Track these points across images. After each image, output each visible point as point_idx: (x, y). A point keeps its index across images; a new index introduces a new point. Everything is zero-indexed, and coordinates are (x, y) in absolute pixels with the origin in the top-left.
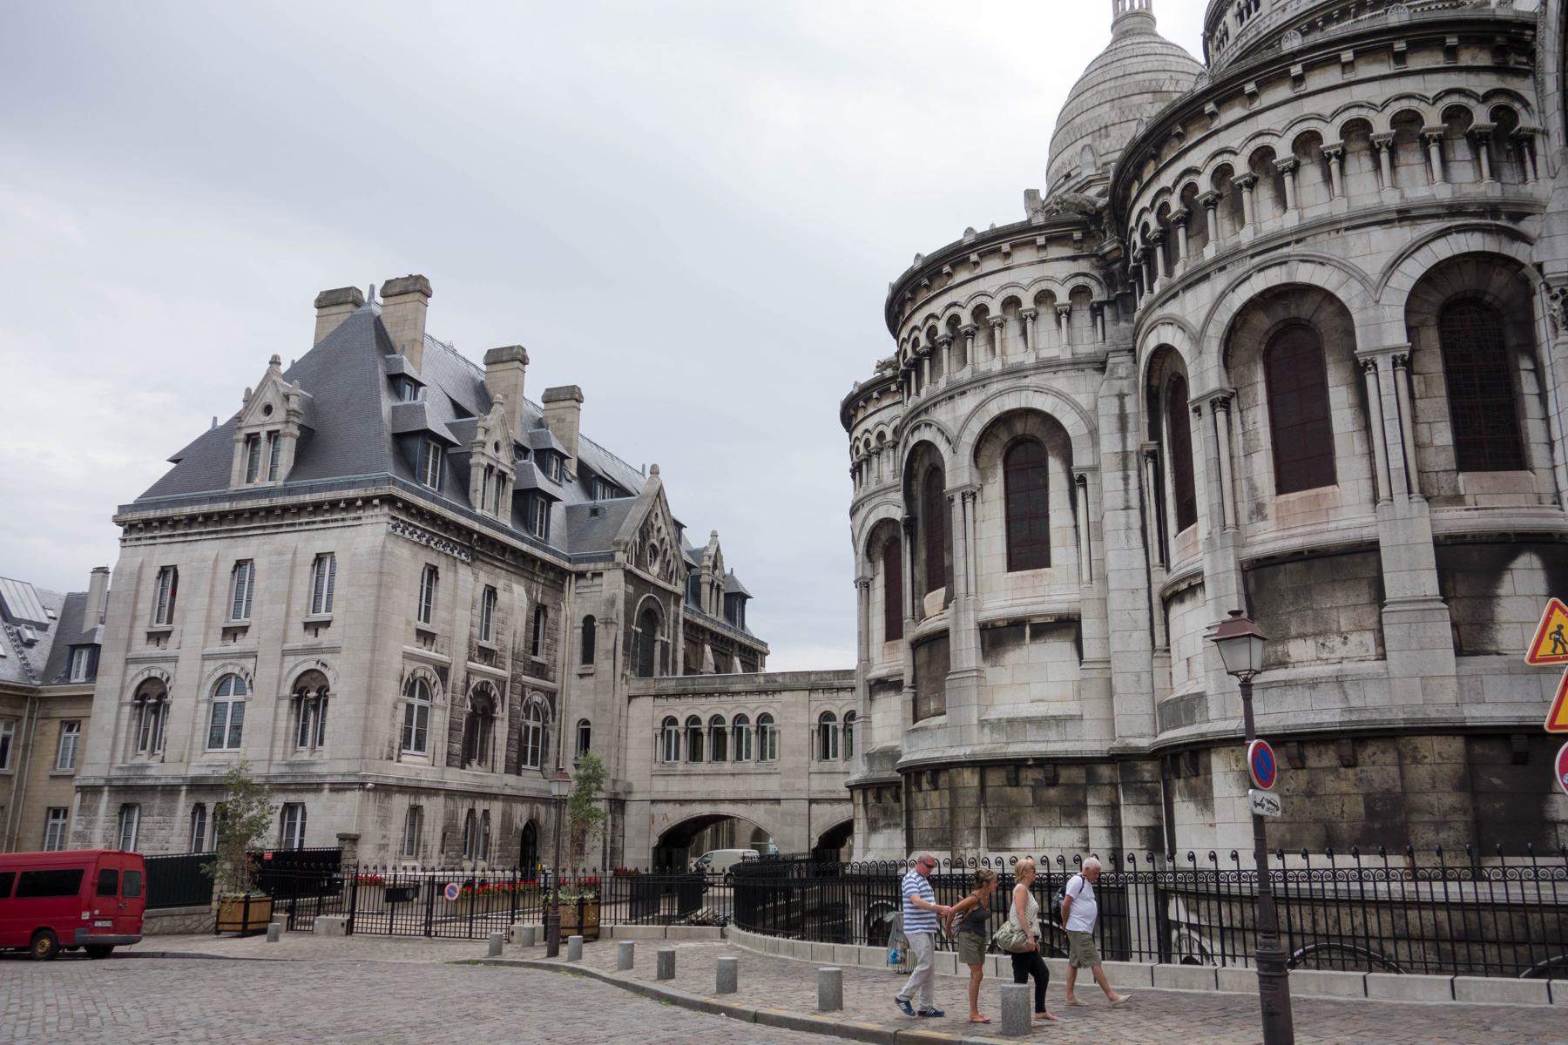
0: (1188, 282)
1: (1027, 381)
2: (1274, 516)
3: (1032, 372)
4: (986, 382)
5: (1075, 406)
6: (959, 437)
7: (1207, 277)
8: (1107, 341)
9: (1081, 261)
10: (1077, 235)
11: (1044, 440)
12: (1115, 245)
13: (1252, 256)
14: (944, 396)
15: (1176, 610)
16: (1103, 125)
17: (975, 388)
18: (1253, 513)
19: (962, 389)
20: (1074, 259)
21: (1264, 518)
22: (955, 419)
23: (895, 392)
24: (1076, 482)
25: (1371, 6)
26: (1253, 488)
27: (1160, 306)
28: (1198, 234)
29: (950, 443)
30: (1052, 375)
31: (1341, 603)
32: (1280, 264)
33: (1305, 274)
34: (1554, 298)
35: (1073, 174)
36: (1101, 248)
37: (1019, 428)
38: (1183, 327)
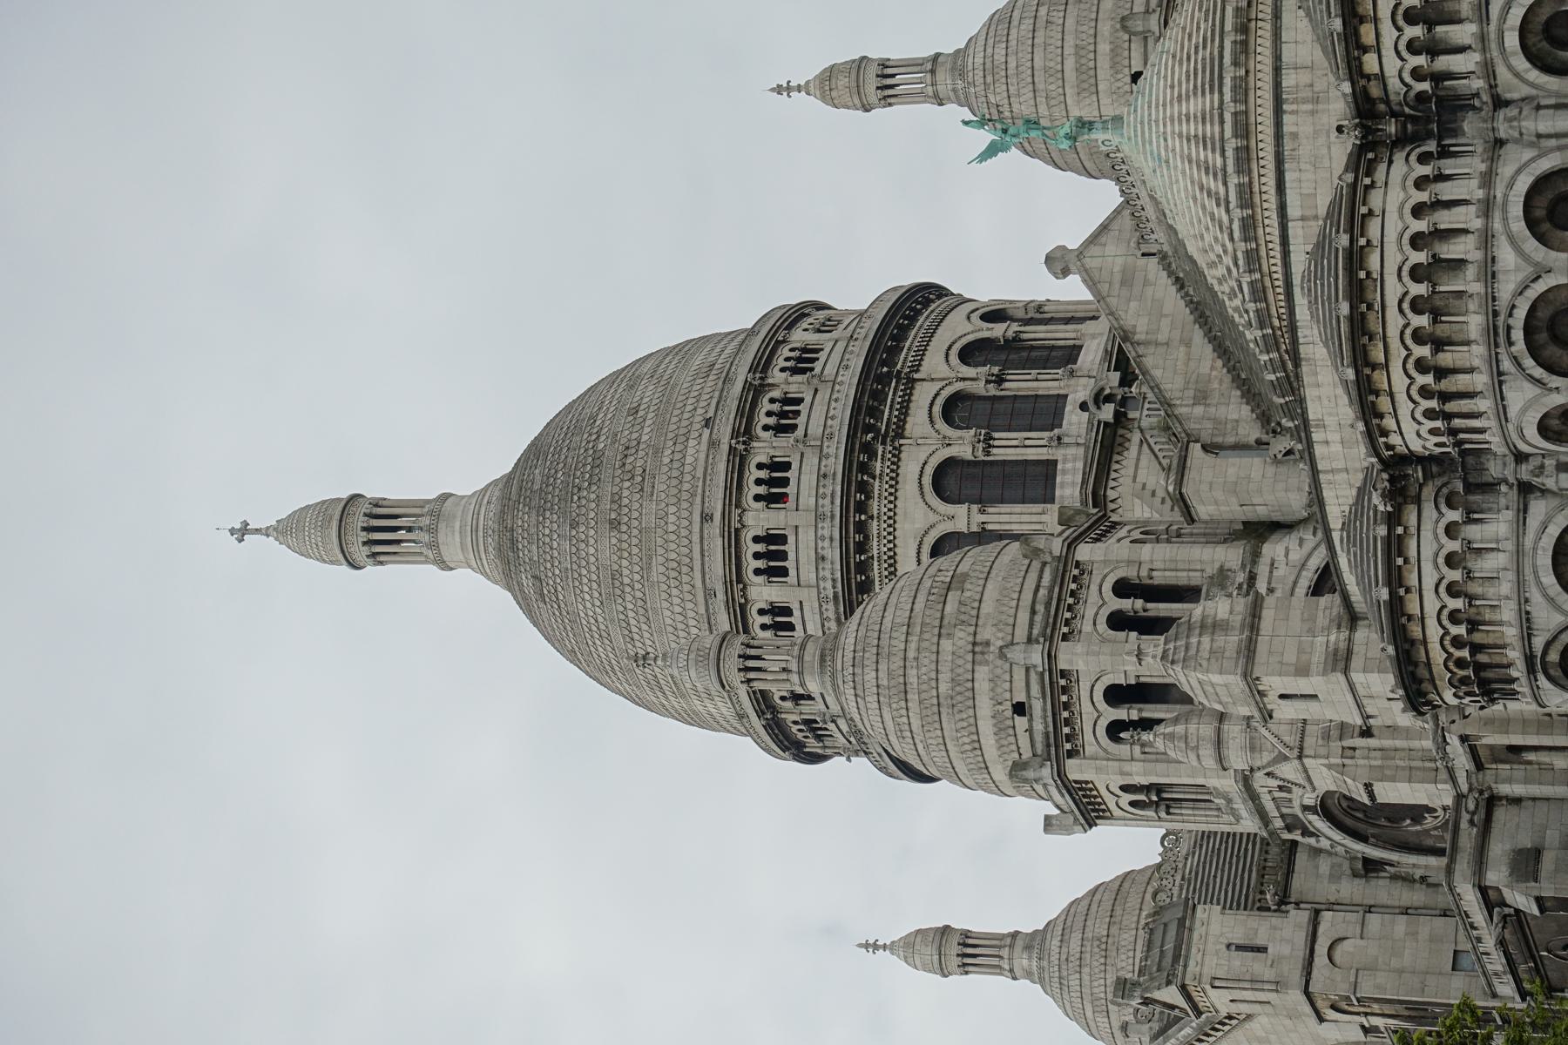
1: (1499, 195)
3: (1492, 192)
4: (1490, 233)
5: (1533, 160)
6: (1537, 264)
8: (1475, 142)
9: (1394, 158)
10: (1371, 155)
11: (1557, 192)
12: (1393, 120)
14: (1489, 284)
16: (970, 647)
17: (1492, 245)
19: (1489, 260)
20: (1390, 162)
22: (1517, 269)
23: (1405, 532)
25: (870, 459)
29: (1539, 277)
30: (1498, 177)
35: (1020, 697)
36: (1390, 135)
37: (1540, 213)
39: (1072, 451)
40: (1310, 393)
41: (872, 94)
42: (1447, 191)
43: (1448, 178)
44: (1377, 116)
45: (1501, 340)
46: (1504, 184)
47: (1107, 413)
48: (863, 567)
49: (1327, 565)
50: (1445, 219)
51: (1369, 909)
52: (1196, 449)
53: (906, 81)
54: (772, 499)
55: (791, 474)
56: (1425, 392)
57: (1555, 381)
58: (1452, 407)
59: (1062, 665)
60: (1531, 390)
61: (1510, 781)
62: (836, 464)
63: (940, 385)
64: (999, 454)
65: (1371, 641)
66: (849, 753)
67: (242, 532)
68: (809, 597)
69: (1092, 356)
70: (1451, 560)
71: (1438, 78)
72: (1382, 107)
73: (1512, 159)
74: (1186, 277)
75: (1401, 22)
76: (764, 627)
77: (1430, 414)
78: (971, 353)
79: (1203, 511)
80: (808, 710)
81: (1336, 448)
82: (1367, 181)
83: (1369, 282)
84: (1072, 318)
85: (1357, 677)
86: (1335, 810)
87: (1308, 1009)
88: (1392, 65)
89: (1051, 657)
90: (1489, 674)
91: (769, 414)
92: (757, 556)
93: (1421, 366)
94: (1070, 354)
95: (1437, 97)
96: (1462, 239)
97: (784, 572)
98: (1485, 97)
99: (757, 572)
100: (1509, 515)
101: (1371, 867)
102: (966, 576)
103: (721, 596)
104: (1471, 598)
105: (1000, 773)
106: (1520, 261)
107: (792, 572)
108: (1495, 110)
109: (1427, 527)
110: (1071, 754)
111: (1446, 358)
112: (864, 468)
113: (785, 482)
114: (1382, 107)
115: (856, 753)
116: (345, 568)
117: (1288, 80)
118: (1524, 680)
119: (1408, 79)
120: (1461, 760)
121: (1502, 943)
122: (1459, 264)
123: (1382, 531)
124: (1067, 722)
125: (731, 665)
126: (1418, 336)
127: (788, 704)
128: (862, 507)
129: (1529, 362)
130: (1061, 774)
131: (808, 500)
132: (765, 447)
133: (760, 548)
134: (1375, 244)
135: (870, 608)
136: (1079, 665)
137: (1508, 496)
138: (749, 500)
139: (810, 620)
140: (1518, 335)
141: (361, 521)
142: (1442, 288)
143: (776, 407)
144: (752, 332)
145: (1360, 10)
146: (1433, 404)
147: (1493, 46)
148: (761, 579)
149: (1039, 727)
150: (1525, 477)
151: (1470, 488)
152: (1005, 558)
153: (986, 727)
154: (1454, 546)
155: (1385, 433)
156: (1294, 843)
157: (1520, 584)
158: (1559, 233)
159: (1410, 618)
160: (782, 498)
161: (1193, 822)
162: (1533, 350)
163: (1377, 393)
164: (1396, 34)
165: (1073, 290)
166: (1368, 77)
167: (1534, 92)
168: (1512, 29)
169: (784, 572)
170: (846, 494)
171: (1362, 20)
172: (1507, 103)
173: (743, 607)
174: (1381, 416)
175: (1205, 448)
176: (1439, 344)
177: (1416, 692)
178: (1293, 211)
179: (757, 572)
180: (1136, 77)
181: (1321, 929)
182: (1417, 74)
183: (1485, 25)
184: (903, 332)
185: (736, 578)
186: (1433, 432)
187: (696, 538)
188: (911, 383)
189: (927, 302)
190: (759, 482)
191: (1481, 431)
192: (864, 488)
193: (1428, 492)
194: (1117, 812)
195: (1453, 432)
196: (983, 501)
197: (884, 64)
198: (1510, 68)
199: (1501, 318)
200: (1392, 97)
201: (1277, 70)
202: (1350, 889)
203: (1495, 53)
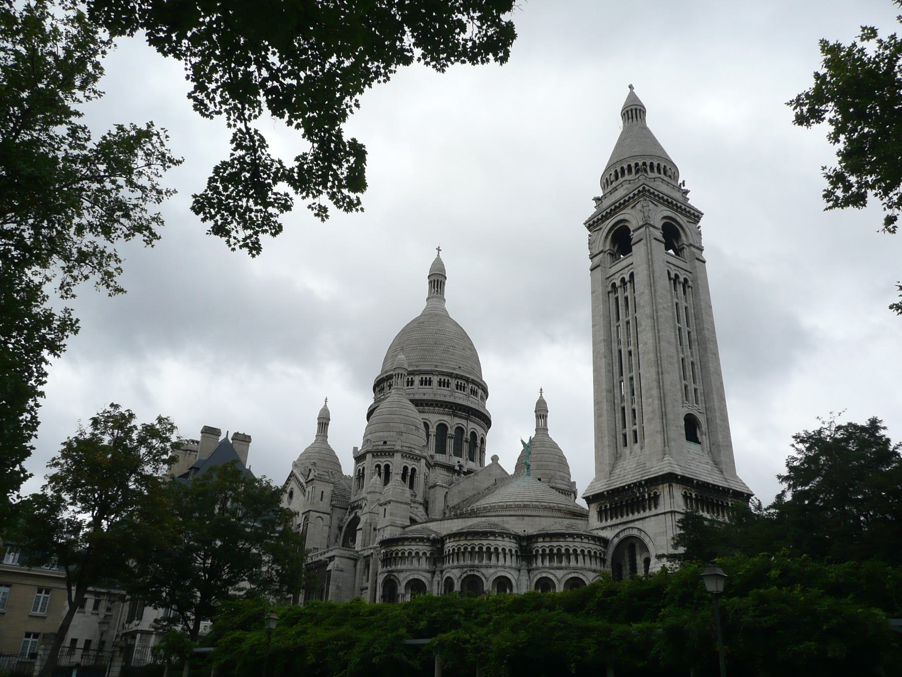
7: (562, 569)
22: (488, 573)
33: (581, 576)
38: (555, 576)
39: (448, 458)
40: (460, 520)
41: (539, 413)
42: (508, 557)
45: (472, 569)
47: (457, 468)
48: (422, 405)
49: (417, 522)
50: (501, 556)
51: (330, 527)
52: (447, 490)
53: (542, 421)
54: (440, 383)
55: (446, 388)
56: (459, 549)
57: (460, 582)
58: (455, 555)
59: (395, 454)
60: (458, 575)
61: (361, 565)
62: (447, 399)
63: (466, 426)
64: (448, 440)
65: (397, 533)
66: (375, 399)
67: (439, 250)
68: (416, 390)
69: (471, 465)
70: (417, 553)
71: (536, 556)
72: (529, 542)
73: (516, 574)
74: (489, 490)
76: (408, 379)
77: (454, 550)
78: (474, 435)
79: (432, 491)
80: (387, 389)
81: (446, 526)
84: (481, 461)
85: (389, 528)
86: (356, 520)
87: (306, 511)
88: (540, 545)
89: (397, 451)
90: (388, 561)
91: (461, 383)
92: (426, 378)
93: (466, 548)
94: (472, 459)
97: (422, 385)
98: (531, 567)
99: (422, 378)
100: (428, 568)
101: (340, 528)
102: (419, 431)
103: (416, 369)
104: (408, 557)
105: (369, 437)
107: (421, 387)
109: (424, 547)
110: (373, 455)
111: (467, 555)
112: (446, 407)
113: (444, 386)
115: (375, 400)
116: (428, 274)
117: (537, 519)
118: (386, 570)
120: (366, 553)
121: (321, 560)
122: (490, 559)
123: (425, 536)
124: (381, 454)
125: (400, 371)
126: (473, 548)
127: (388, 384)
128: (437, 405)
129: (465, 575)
130: (368, 452)
131: (439, 392)
132: (453, 382)
133: (428, 379)
135: (412, 406)
136: (395, 458)
137: (432, 568)
138: (440, 377)
139: (409, 390)
140: (472, 573)
141: (440, 279)
143: (463, 385)
144: (481, 379)
146: (456, 551)
148: (420, 379)
149: (380, 447)
150: (437, 572)
151: (434, 559)
152: (423, 441)
153: (381, 434)
154: (421, 554)
155: (450, 538)
156: (347, 509)
157: (411, 570)
159: (404, 542)
160: (440, 386)
161: (354, 484)
162: (468, 576)
163: (460, 537)
165: (488, 461)
166: (537, 539)
169: (422, 385)
170: (440, 401)
171: (551, 538)
173: (413, 374)
174: (454, 538)
175: (447, 493)
176: (470, 553)
177: (385, 543)
178: (505, 518)
179: (422, 378)
180: (540, 479)
181: (326, 515)
182: (537, 551)
184: (480, 418)
185: (420, 373)
186: (449, 550)
187: (431, 363)
188: (467, 419)
189: (486, 424)
190: (444, 380)
191: (449, 562)
192: (441, 406)
193: (435, 548)
194: (358, 465)
195: (449, 555)
196: (436, 436)
197: (546, 416)
198: (537, 574)
199: (476, 569)
201: (539, 516)
202: (335, 522)
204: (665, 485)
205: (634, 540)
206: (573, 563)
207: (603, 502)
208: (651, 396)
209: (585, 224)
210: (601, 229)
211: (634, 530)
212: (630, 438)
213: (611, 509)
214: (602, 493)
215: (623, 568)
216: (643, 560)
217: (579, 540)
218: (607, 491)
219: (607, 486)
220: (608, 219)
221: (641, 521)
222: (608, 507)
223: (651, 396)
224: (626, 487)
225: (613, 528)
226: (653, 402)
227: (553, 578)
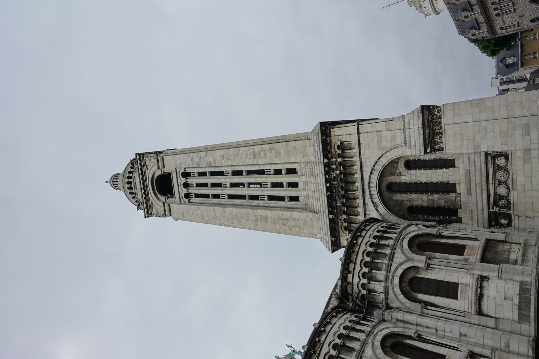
0: (391, 259)
1: (375, 332)
2: (469, 256)
3: (373, 330)
4: (366, 342)
7: (394, 253)
10: (340, 310)
12: (352, 302)
13: (398, 242)
15: (485, 309)
17: (365, 346)
18: (466, 261)
20: (346, 314)
21: (469, 259)
24: (420, 338)
26: (458, 260)
27: (390, 273)
28: (379, 258)
31: (502, 247)
32: (404, 238)
33: (410, 236)
34: (439, 225)
36: (349, 307)
37: (388, 344)
43: (362, 324)
44: (348, 300)
46: (379, 330)
71: (370, 291)
72: (350, 297)
75: (362, 265)
82: (335, 314)
83: (318, 344)
95: (369, 300)
96: (357, 342)
98: (384, 304)
106: (373, 355)
108: (386, 309)
114: (350, 297)
119: (360, 288)
134: (326, 332)
142: (342, 356)
145: (352, 259)
147: (390, 281)
158: (392, 353)
164: (360, 269)
166: (348, 283)
167: (400, 305)
168: (397, 276)
171: (351, 262)
172: (391, 308)
183: (388, 273)
200: (354, 294)
203: (390, 284)
204: (332, 134)
205: (384, 185)
206: (391, 242)
207: (340, 224)
208: (259, 152)
209: (145, 218)
210: (152, 202)
211: (372, 180)
212: (293, 192)
213: (348, 215)
214: (331, 221)
215: (415, 203)
216: (407, 171)
217: (364, 232)
218: (330, 213)
219: (325, 216)
220: (148, 194)
221: (364, 169)
222: (345, 216)
223: (259, 152)
224: (328, 185)
225: (367, 213)
226: (264, 151)
227: (404, 267)
